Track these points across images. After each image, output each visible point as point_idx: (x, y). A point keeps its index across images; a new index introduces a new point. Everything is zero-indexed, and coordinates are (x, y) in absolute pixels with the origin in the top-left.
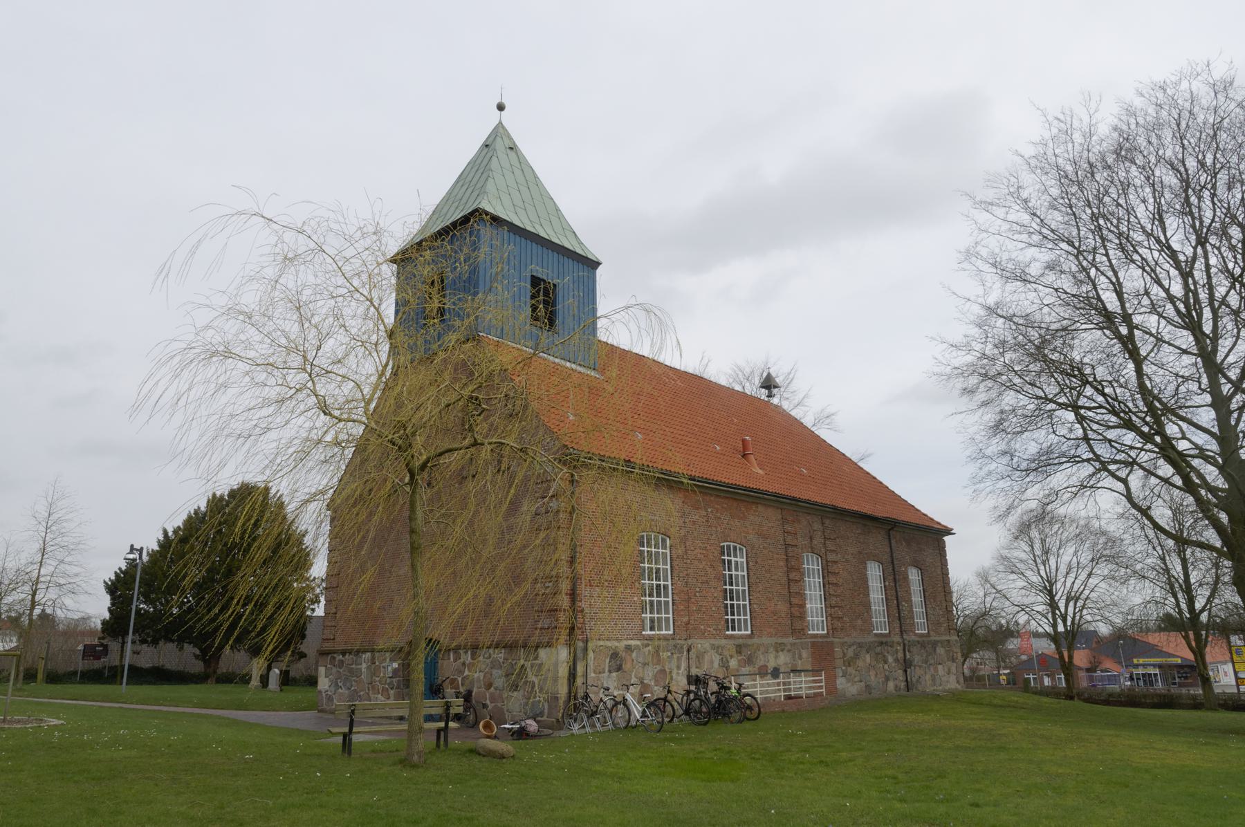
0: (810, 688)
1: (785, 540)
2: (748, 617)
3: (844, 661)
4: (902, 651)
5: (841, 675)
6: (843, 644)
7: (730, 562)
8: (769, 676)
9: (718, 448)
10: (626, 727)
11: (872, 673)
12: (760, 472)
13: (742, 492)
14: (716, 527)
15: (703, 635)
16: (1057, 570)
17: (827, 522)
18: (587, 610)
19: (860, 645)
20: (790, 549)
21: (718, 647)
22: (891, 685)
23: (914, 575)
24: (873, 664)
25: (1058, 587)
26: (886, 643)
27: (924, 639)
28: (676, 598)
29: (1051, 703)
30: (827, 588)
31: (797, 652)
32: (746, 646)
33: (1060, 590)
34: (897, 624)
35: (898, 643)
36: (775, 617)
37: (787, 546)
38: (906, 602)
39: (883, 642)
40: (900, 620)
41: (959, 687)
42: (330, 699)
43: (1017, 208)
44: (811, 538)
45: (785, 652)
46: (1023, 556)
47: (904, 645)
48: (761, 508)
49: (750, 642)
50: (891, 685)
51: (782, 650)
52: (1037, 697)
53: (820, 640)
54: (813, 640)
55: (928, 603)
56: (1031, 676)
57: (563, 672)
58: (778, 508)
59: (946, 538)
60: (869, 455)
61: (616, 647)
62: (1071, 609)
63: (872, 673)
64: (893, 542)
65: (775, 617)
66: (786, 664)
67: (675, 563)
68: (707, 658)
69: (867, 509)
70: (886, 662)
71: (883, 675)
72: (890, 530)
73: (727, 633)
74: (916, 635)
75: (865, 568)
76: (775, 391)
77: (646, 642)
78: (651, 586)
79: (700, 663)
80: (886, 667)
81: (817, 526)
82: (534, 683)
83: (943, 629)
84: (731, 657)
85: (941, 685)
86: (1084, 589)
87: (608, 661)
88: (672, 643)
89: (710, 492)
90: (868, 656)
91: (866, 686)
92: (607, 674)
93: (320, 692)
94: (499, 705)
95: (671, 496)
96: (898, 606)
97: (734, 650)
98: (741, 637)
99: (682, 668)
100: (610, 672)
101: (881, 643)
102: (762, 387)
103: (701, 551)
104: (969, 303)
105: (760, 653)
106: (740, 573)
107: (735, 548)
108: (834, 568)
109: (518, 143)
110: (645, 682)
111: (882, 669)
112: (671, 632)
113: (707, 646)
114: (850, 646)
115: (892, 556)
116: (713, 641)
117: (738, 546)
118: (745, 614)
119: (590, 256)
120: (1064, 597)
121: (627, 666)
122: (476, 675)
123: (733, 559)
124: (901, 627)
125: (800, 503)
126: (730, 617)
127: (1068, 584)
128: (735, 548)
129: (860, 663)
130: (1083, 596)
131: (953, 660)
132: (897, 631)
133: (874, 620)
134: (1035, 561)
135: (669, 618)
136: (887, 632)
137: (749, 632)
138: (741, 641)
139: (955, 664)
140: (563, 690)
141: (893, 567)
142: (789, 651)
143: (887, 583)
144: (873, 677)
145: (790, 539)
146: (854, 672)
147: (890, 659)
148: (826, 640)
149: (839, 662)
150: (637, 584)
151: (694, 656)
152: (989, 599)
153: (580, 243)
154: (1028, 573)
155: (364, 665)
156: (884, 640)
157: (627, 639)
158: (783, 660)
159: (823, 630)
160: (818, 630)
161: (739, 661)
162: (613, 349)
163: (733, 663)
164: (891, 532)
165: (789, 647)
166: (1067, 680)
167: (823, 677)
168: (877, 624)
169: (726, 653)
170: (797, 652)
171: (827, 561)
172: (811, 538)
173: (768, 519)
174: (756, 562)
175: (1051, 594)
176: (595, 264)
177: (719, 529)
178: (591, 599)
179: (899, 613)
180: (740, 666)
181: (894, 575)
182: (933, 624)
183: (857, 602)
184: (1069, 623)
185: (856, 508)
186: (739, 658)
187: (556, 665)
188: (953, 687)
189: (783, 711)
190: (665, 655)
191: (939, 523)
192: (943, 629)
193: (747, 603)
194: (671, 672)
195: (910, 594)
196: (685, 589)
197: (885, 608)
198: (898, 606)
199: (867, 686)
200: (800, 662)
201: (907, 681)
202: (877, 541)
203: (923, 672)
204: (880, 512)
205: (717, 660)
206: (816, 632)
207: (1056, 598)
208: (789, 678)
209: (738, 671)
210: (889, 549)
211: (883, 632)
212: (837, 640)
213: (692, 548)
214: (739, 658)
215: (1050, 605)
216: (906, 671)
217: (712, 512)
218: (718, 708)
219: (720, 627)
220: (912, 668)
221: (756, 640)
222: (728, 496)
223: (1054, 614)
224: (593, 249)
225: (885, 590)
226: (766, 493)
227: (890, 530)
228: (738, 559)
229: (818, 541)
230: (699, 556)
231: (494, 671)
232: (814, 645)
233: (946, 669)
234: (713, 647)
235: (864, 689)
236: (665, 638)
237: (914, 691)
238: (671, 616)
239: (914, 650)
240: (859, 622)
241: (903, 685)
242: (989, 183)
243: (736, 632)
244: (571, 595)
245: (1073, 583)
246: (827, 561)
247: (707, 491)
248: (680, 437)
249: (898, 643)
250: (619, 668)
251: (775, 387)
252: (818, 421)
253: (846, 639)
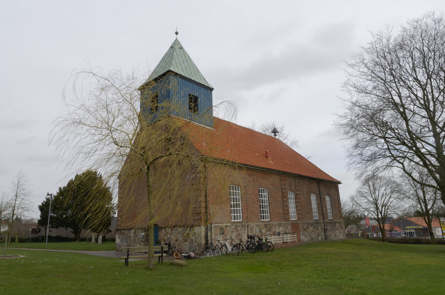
0: (291, 239)
1: (281, 187)
2: (269, 214)
3: (303, 230)
4: (324, 225)
5: (302, 234)
6: (303, 223)
7: (262, 195)
8: (277, 235)
9: (257, 154)
10: (226, 254)
11: (313, 233)
12: (272, 163)
13: (266, 170)
14: (257, 183)
15: (253, 221)
16: (378, 196)
17: (296, 180)
18: (211, 213)
19: (309, 224)
20: (283, 190)
21: (258, 225)
22: (320, 238)
23: (327, 198)
24: (313, 230)
25: (379, 202)
26: (318, 223)
27: (331, 221)
28: (243, 208)
29: (377, 243)
30: (297, 203)
31: (286, 226)
32: (268, 225)
33: (380, 202)
34: (322, 216)
35: (322, 223)
36: (278, 214)
37: (282, 189)
38: (325, 208)
39: (317, 222)
40: (323, 214)
41: (344, 238)
42: (120, 246)
43: (363, 66)
44: (291, 186)
45: (282, 226)
46: (366, 191)
47: (324, 223)
48: (272, 176)
49: (270, 223)
50: (320, 238)
51: (281, 226)
52: (372, 241)
53: (294, 222)
54: (292, 222)
55: (332, 208)
56: (369, 233)
57: (203, 235)
58: (279, 175)
59: (339, 185)
60: (311, 157)
61: (222, 226)
62: (383, 209)
63: (313, 233)
64: (320, 187)
65: (278, 214)
66: (282, 231)
67: (242, 196)
68: (254, 229)
69: (311, 175)
70: (318, 229)
72: (319, 182)
73: (261, 220)
74: (328, 219)
75: (310, 196)
76: (277, 134)
77: (233, 224)
78: (234, 204)
79: (252, 231)
80: (318, 231)
81: (293, 182)
82: (193, 240)
83: (338, 217)
84: (263, 229)
85: (337, 237)
86: (388, 202)
87: (219, 231)
88: (242, 224)
89: (254, 170)
90: (312, 228)
92: (219, 236)
93: (117, 244)
94: (180, 247)
95: (241, 172)
96: (322, 210)
97: (264, 226)
98: (266, 221)
99: (246, 233)
100: (220, 235)
101: (317, 223)
102: (272, 132)
103: (251, 191)
104: (346, 101)
105: (273, 227)
106: (265, 199)
107: (264, 190)
108: (299, 197)
109: (183, 46)
110: (233, 238)
112: (241, 220)
113: (254, 225)
114: (305, 224)
115: (320, 192)
116: (256, 223)
117: (265, 189)
118: (268, 213)
119: (210, 86)
120: (381, 205)
121: (226, 233)
122: (172, 237)
123: (263, 194)
124: (323, 217)
125: (287, 174)
126: (262, 215)
127: (382, 201)
128: (264, 190)
129: (309, 230)
130: (388, 205)
131: (342, 228)
132: (322, 218)
133: (314, 214)
134: (371, 193)
135: (240, 215)
136: (318, 219)
137: (269, 220)
138: (266, 223)
140: (203, 241)
141: (320, 195)
142: (283, 226)
143: (318, 202)
144: (313, 235)
145: (283, 186)
147: (320, 228)
148: (296, 222)
149: (301, 230)
150: (229, 204)
151: (250, 229)
152: (354, 207)
153: (206, 82)
154: (368, 197)
155: (132, 234)
156: (317, 222)
157: (226, 223)
158: (281, 229)
159: (296, 218)
160: (294, 218)
161: (266, 230)
162: (218, 120)
163: (264, 231)
164: (319, 183)
165: (283, 225)
166: (382, 235)
167: (296, 235)
168: (315, 216)
169: (261, 227)
170: (286, 226)
171: (296, 194)
172: (291, 186)
173: (275, 179)
174: (271, 195)
175: (376, 204)
176: (212, 89)
177: (258, 183)
178: (212, 209)
179: (322, 212)
180: (266, 232)
181: (321, 198)
182: (334, 216)
184: (383, 214)
185: (306, 175)
186: (266, 229)
187: (201, 233)
188: (342, 238)
189: (282, 247)
190: (239, 228)
191: (336, 180)
192: (338, 217)
193: (268, 209)
194: (241, 235)
195: (326, 205)
196: (246, 205)
197: (317, 210)
198: (322, 210)
199: (311, 238)
200: (287, 230)
201: (325, 236)
202: (314, 186)
203: (331, 233)
204: (315, 176)
205: (258, 230)
206: (293, 219)
207: (378, 206)
208: (284, 236)
209: (265, 233)
210: (318, 190)
211: (317, 219)
212: (301, 222)
213: (248, 190)
214: (266, 229)
215: (376, 208)
216: (325, 233)
217: (255, 177)
218: (259, 247)
219: (259, 218)
220: (327, 231)
221: (272, 223)
222: (262, 171)
223: (377, 212)
224: (211, 84)
225: (317, 204)
226: (274, 170)
227: (319, 182)
228: (265, 194)
229: (293, 187)
230: (251, 193)
231: (179, 236)
232: (292, 224)
233: (339, 232)
234: (256, 225)
236: (239, 222)
238: (241, 214)
239: (328, 225)
240: (308, 215)
241: (324, 237)
242: (353, 58)
243: (265, 220)
244: (205, 208)
245: (384, 200)
246: (296, 194)
247: (253, 170)
248: (243, 151)
249: (322, 223)
250: (223, 233)
251: (277, 132)
252: (292, 144)
253: (304, 222)
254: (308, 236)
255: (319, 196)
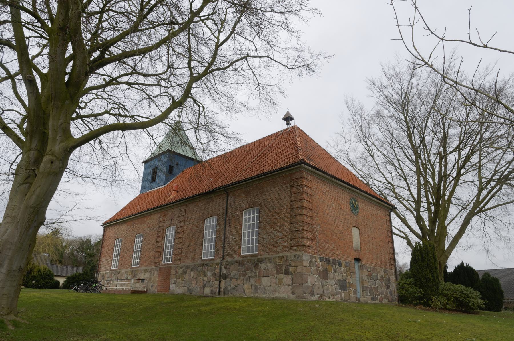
5: (173, 283)
19: (188, 267)
22: (207, 290)
26: (207, 265)
27: (245, 259)
34: (221, 252)
38: (233, 235)
39: (206, 264)
50: (207, 290)
53: (166, 266)
63: (194, 283)
71: (202, 284)
80: (205, 279)
90: (192, 274)
91: (188, 289)
111: (202, 280)
113: (124, 271)
114: (181, 268)
129: (187, 277)
131: (287, 273)
139: (290, 277)
142: (149, 272)
144: (194, 285)
146: (181, 281)
147: (209, 274)
165: (150, 270)
183: (192, 244)
188: (282, 296)
200: (153, 276)
216: (220, 282)
220: (228, 279)
235: (187, 291)
237: (230, 295)
240: (192, 254)
254: (182, 285)
255: (224, 217)
